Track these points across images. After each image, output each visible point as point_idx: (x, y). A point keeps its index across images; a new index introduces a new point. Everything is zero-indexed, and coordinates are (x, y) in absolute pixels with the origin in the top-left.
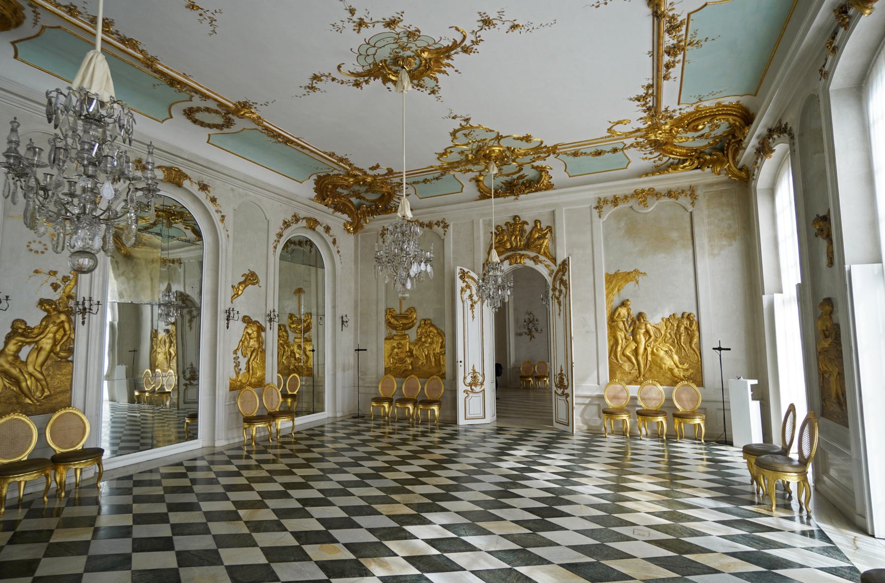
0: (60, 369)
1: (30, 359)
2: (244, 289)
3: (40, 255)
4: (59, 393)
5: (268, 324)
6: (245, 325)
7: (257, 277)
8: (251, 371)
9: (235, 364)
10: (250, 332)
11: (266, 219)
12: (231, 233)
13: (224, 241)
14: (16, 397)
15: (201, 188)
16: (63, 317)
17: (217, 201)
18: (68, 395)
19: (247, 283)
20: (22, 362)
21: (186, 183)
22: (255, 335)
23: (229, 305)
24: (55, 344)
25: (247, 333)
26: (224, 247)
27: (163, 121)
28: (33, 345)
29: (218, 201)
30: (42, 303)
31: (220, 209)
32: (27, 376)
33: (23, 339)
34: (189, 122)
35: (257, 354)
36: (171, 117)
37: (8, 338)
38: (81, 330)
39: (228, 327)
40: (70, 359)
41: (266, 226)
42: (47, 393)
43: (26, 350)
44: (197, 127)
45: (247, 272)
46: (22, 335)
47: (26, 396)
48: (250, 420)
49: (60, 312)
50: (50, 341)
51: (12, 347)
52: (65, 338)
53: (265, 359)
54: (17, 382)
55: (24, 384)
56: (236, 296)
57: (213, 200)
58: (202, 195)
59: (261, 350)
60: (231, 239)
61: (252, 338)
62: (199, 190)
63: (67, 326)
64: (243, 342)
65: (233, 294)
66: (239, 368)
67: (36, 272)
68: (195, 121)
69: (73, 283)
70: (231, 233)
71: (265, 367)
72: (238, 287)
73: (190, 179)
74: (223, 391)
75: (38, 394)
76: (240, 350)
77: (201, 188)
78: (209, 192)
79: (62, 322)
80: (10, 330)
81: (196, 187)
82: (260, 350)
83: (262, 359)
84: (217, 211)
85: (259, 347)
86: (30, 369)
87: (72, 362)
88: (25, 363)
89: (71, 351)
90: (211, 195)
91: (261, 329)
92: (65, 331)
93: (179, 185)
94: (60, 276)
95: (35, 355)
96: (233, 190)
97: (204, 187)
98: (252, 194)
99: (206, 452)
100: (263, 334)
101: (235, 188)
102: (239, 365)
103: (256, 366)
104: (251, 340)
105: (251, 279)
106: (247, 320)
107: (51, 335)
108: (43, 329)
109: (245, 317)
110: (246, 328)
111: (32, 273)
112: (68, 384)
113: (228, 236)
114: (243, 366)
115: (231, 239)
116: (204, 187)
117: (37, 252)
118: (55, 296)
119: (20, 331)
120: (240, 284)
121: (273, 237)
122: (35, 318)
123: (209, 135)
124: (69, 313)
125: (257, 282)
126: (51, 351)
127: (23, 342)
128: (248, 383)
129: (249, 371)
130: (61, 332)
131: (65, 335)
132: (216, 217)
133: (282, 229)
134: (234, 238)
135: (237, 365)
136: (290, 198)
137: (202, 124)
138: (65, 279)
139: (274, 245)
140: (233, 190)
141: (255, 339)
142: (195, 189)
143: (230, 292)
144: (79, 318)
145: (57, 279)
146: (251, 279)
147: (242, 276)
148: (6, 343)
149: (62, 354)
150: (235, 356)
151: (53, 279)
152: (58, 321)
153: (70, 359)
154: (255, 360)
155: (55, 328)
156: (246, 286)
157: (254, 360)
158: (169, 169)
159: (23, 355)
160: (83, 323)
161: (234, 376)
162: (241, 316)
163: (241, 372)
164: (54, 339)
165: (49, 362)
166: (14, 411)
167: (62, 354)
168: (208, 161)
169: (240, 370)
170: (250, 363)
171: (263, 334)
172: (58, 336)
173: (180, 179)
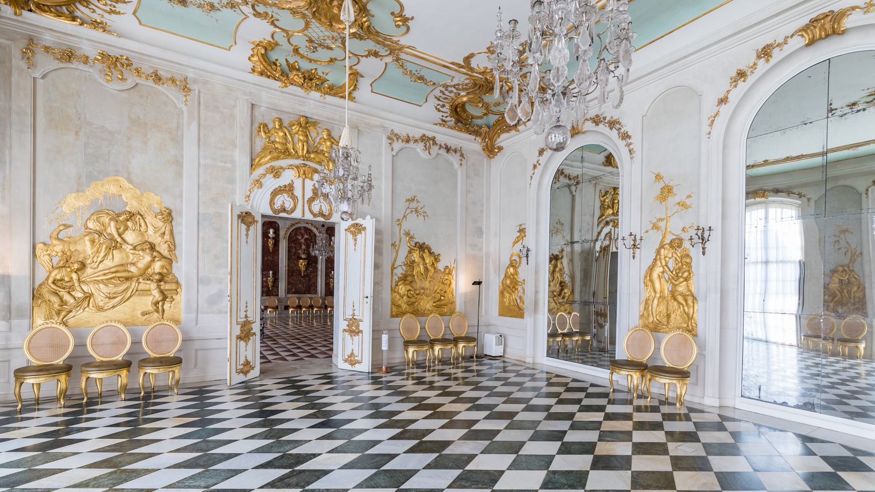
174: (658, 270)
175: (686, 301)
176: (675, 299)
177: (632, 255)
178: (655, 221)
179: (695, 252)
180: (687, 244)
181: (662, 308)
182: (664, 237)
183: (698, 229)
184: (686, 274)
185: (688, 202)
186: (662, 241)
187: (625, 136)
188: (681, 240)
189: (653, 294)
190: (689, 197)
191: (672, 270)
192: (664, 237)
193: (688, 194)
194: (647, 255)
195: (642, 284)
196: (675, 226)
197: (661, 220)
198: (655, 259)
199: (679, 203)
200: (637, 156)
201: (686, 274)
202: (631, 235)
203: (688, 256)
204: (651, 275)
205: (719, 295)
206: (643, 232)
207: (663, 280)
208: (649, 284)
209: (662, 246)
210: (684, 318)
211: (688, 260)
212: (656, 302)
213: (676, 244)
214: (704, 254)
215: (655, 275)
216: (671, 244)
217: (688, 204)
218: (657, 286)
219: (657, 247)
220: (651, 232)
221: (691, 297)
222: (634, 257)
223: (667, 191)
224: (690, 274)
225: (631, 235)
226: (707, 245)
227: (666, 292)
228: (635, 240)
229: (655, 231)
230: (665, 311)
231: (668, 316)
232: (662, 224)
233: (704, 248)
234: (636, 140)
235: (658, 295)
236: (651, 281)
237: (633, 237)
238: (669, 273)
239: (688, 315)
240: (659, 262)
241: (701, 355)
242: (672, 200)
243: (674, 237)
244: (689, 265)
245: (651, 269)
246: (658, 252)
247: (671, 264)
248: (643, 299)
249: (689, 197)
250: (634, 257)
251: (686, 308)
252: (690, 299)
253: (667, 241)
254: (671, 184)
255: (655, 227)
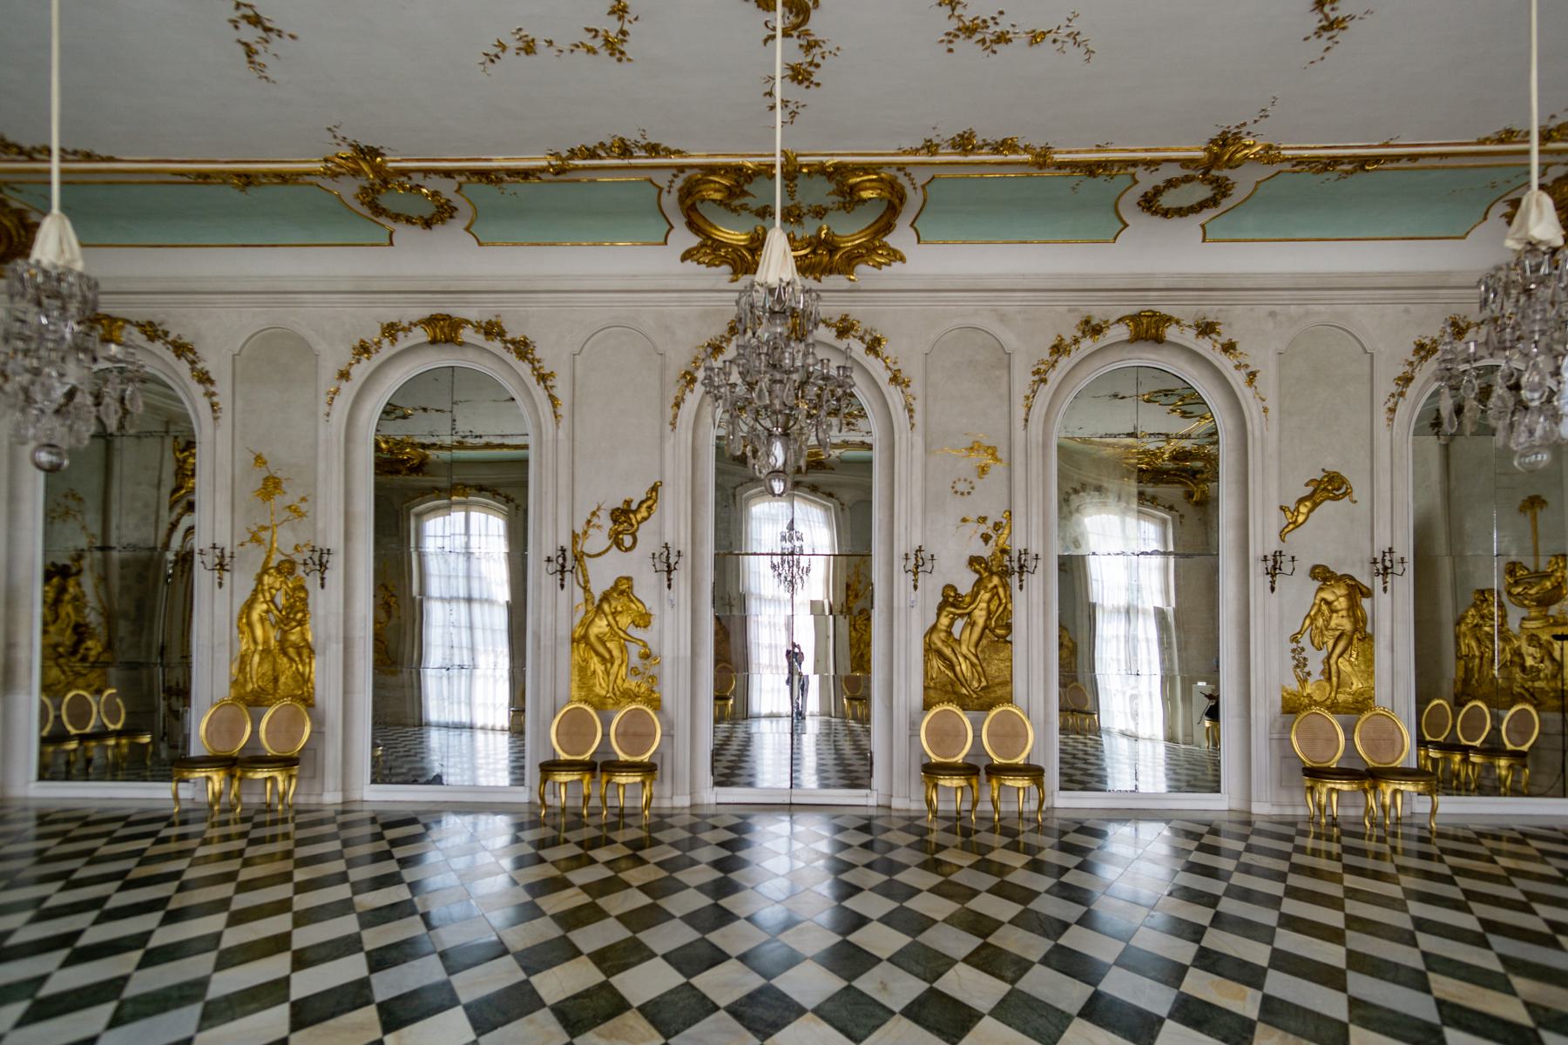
0: (997, 651)
1: (963, 637)
2: (1311, 511)
3: (966, 497)
4: (998, 684)
5: (1379, 580)
6: (1317, 584)
7: (1343, 481)
8: (1334, 679)
9: (1295, 662)
10: (1330, 597)
11: (1366, 352)
12: (1272, 404)
13: (1257, 421)
14: (952, 685)
15: (1200, 333)
16: (996, 580)
17: (1238, 347)
18: (1008, 689)
19: (1318, 498)
20: (955, 640)
21: (1171, 333)
22: (1342, 603)
23: (1273, 545)
24: (989, 618)
25: (1323, 599)
26: (1257, 433)
27: (1115, 238)
28: (966, 619)
29: (1239, 348)
30: (974, 561)
31: (1244, 361)
32: (961, 659)
33: (953, 610)
34: (1157, 219)
35: (1350, 643)
36: (1126, 225)
37: (941, 608)
38: (1019, 598)
39: (1273, 589)
40: (1008, 639)
41: (1367, 369)
42: (984, 684)
43: (959, 623)
44: (1176, 222)
45: (1319, 476)
46: (953, 605)
47: (962, 685)
48: (1316, 774)
49: (992, 574)
50: (984, 613)
51: (945, 621)
52: (1001, 609)
53: (1373, 655)
54: (952, 667)
55: (958, 668)
56: (1291, 526)
57: (1229, 347)
58: (1204, 346)
59: (1360, 634)
60: (1273, 412)
61: (1337, 612)
62: (1197, 336)
63: (1001, 590)
64: (1313, 620)
65: (1286, 523)
66: (1306, 670)
67: (964, 520)
68: (1166, 213)
69: (1006, 532)
70: (1272, 404)
71: (1373, 672)
72: (1297, 509)
73: (1178, 322)
74: (1265, 710)
75: (975, 684)
76: (1307, 635)
77: (1200, 333)
78: (1219, 334)
79: (996, 587)
80: (940, 599)
81: (1191, 333)
82: (1357, 635)
83: (1364, 656)
84: (1237, 367)
85: (1355, 630)
86: (964, 649)
87: (1011, 642)
88: (959, 642)
89: (1009, 627)
90: (1224, 339)
91: (1357, 591)
92: (1000, 599)
93: (1159, 340)
94: (990, 523)
95: (968, 631)
96: (1273, 314)
97: (1206, 329)
98: (1322, 308)
99: (1234, 817)
100: (1365, 603)
101: (1277, 308)
102: (1305, 665)
103: (1349, 669)
104: (1335, 615)
105: (1330, 487)
106: (1323, 575)
107: (984, 605)
108: (974, 595)
109: (1315, 567)
110: (1320, 589)
111: (960, 524)
112: (1007, 673)
113: (1265, 410)
114: (1315, 665)
115: (1273, 412)
116: (1206, 329)
117: (962, 494)
118: (986, 552)
119: (951, 600)
120: (1301, 501)
121: (1386, 387)
122: (965, 582)
123: (1203, 226)
124: (1005, 573)
125: (1345, 494)
126: (985, 627)
127: (954, 614)
128: (1329, 702)
129: (1329, 679)
130: (995, 602)
131: (1000, 604)
132: (1237, 379)
133: (1411, 364)
134: (1281, 412)
135: (1301, 664)
136: (1428, 286)
137: (1181, 212)
138: (997, 526)
139: (1390, 405)
140: (1273, 314)
141: (1344, 613)
142: (1189, 338)
143: (1275, 521)
144: (1014, 581)
145: (986, 528)
146: (1330, 487)
147: (1307, 485)
148: (939, 615)
149: (999, 632)
150: (1294, 645)
151: (983, 529)
152: (990, 586)
153: (1008, 639)
154: (1346, 656)
155: (987, 596)
156: (1316, 505)
157: (1341, 655)
158: (1135, 319)
159: (956, 631)
160: (1021, 587)
161: (1294, 686)
162: (1305, 564)
163: (1311, 680)
164: (989, 612)
165: (984, 642)
166: (950, 701)
167: (999, 632)
168: (1207, 276)
169: (1309, 674)
170: (1332, 661)
171: (1365, 603)
172: (993, 607)
173: (1157, 330)
174: (260, 608)
175: (300, 655)
176: (285, 654)
177: (217, 581)
178: (254, 528)
179: (311, 583)
180: (300, 570)
181: (267, 667)
182: (269, 557)
183: (313, 551)
184: (299, 615)
185: (304, 507)
186: (266, 562)
187: (204, 378)
188: (292, 563)
189: (252, 647)
190: (303, 499)
191: (280, 607)
192: (269, 557)
193: (302, 495)
194: (242, 582)
195: (235, 631)
196: (285, 541)
197: (265, 528)
198: (256, 591)
199: (289, 507)
200: (226, 417)
201: (299, 615)
202: (214, 547)
203: (303, 588)
204: (249, 617)
205: (341, 646)
206: (236, 543)
207: (267, 623)
208: (246, 629)
209: (265, 571)
210: (297, 681)
211: (302, 595)
212: (256, 658)
213: (286, 568)
214: (323, 586)
215: (255, 616)
216: (278, 569)
217: (304, 510)
218: (259, 632)
219: (259, 570)
220: (248, 545)
221: (306, 651)
222: (220, 585)
223: (271, 486)
224: (305, 616)
225: (214, 547)
226: (327, 574)
227: (272, 642)
228: (223, 556)
229: (255, 544)
230: (270, 673)
231: (276, 680)
232: (265, 535)
233: (323, 579)
234: (223, 388)
235: (260, 648)
236: (250, 624)
237: (218, 552)
238: (276, 612)
239: (302, 675)
240: (260, 596)
241: (318, 732)
242: (279, 501)
243: (283, 558)
244: (304, 601)
245: (249, 606)
246: (260, 580)
247: (281, 600)
248: (237, 654)
249: (303, 499)
250: (220, 585)
251: (300, 667)
252: (305, 652)
253: (273, 563)
254: (279, 474)
255: (256, 539)
